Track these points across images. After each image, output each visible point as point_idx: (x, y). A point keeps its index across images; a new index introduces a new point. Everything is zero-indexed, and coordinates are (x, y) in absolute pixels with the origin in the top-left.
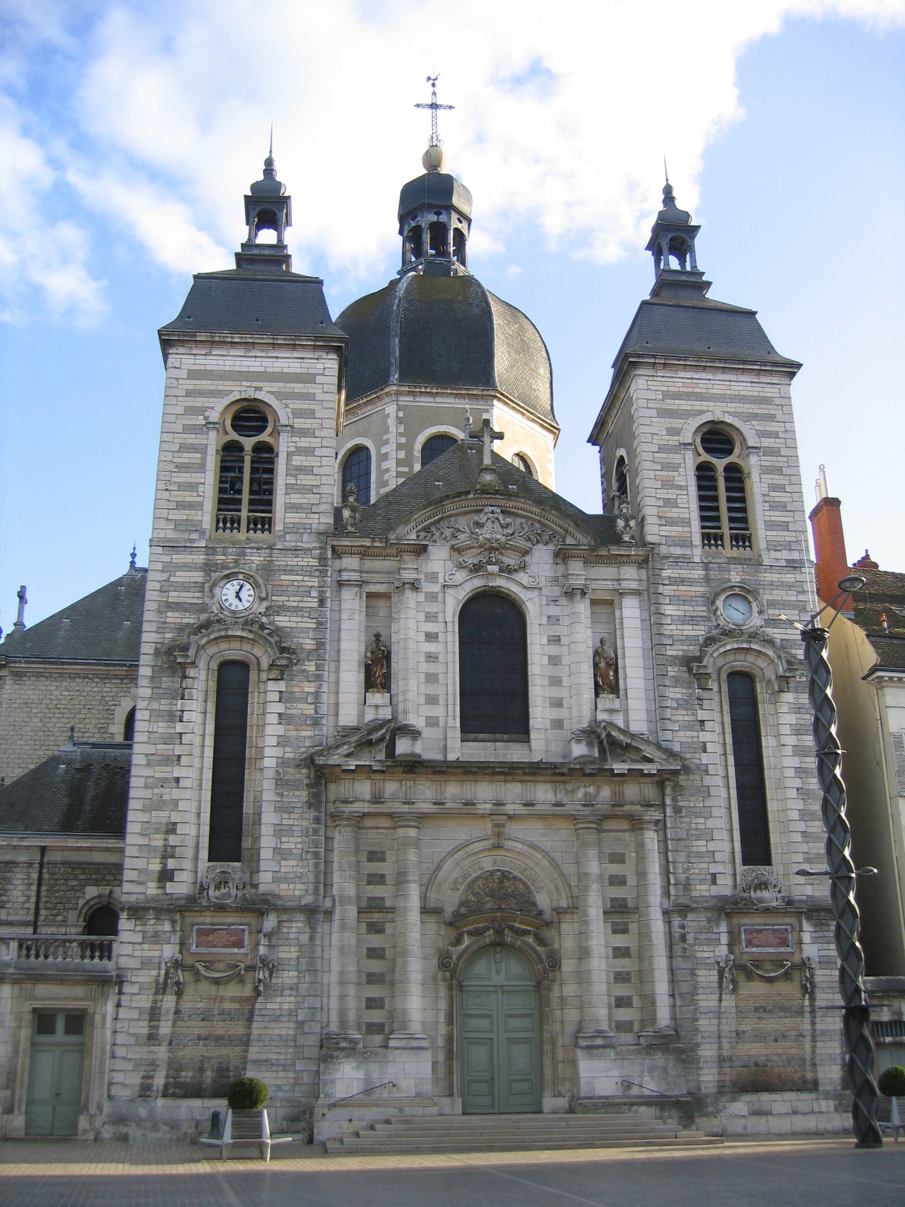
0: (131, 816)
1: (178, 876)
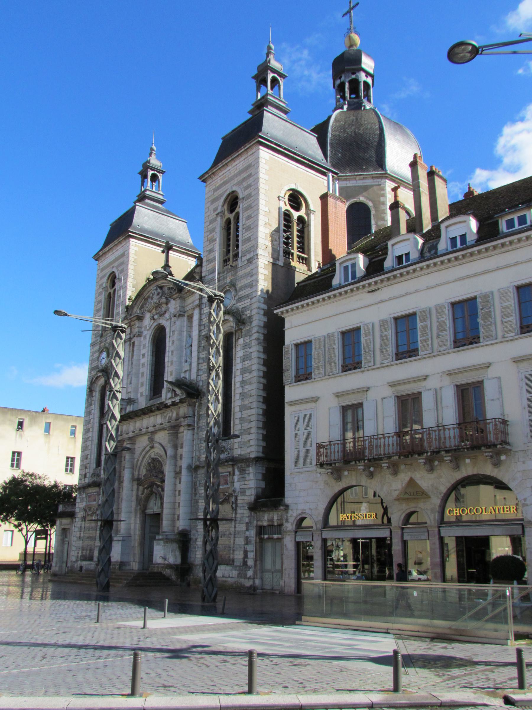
1: (88, 475)
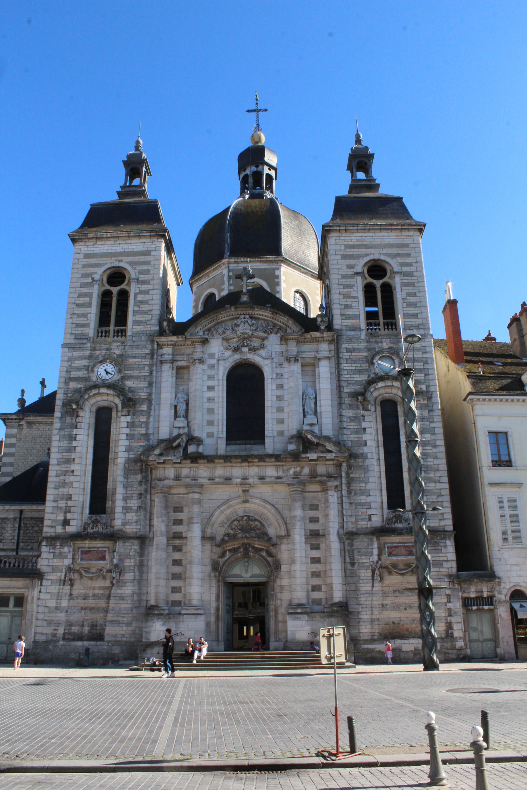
0: (49, 491)
1: (72, 523)
